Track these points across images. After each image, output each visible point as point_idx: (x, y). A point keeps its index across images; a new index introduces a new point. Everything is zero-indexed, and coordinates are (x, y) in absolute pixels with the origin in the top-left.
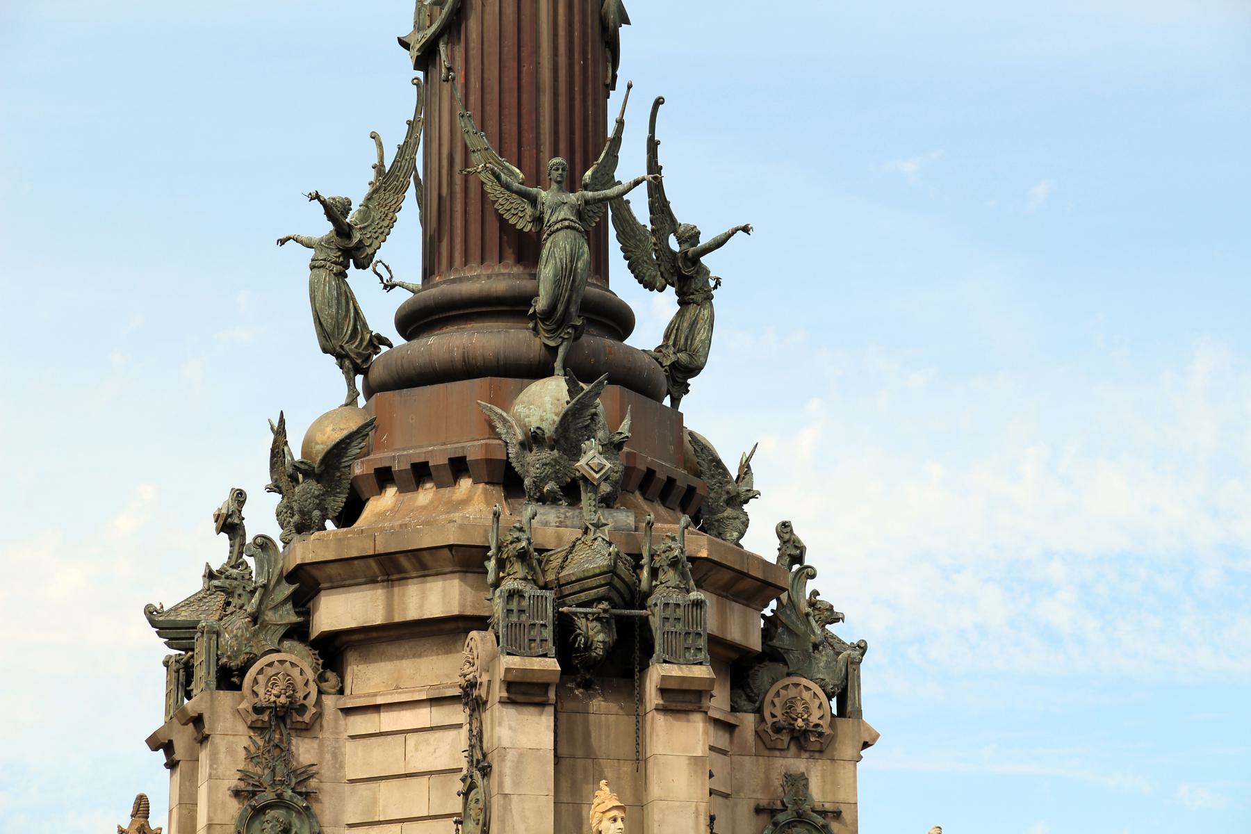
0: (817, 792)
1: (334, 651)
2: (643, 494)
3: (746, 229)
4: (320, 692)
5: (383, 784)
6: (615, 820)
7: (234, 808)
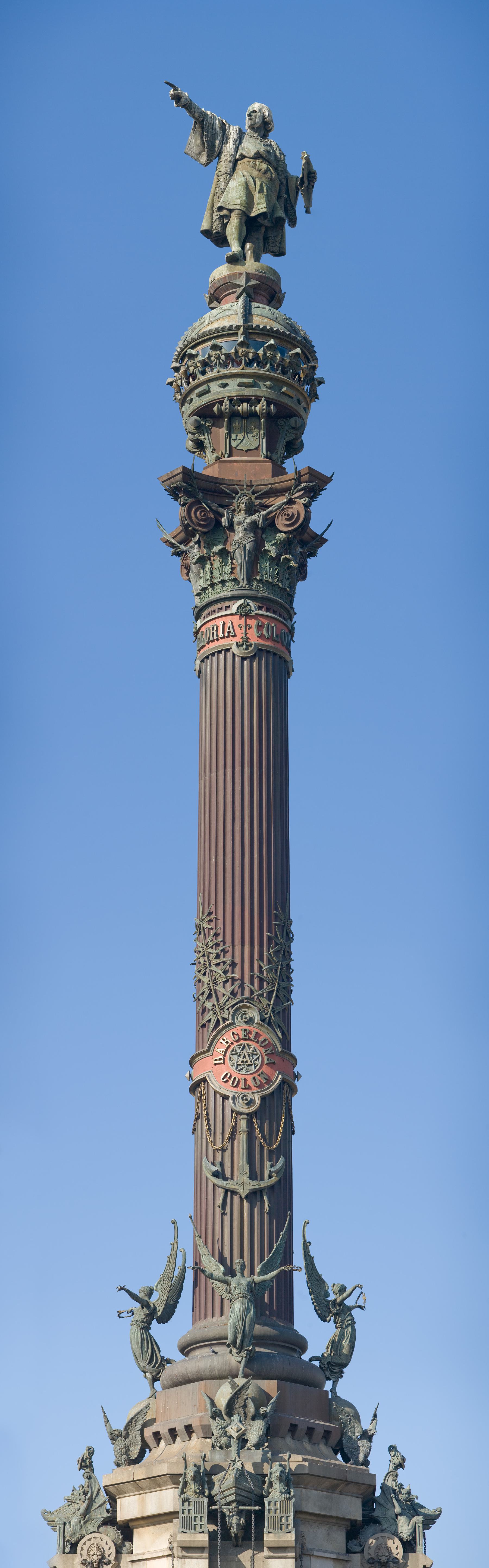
2: (293, 1437)
4: (118, 1552)
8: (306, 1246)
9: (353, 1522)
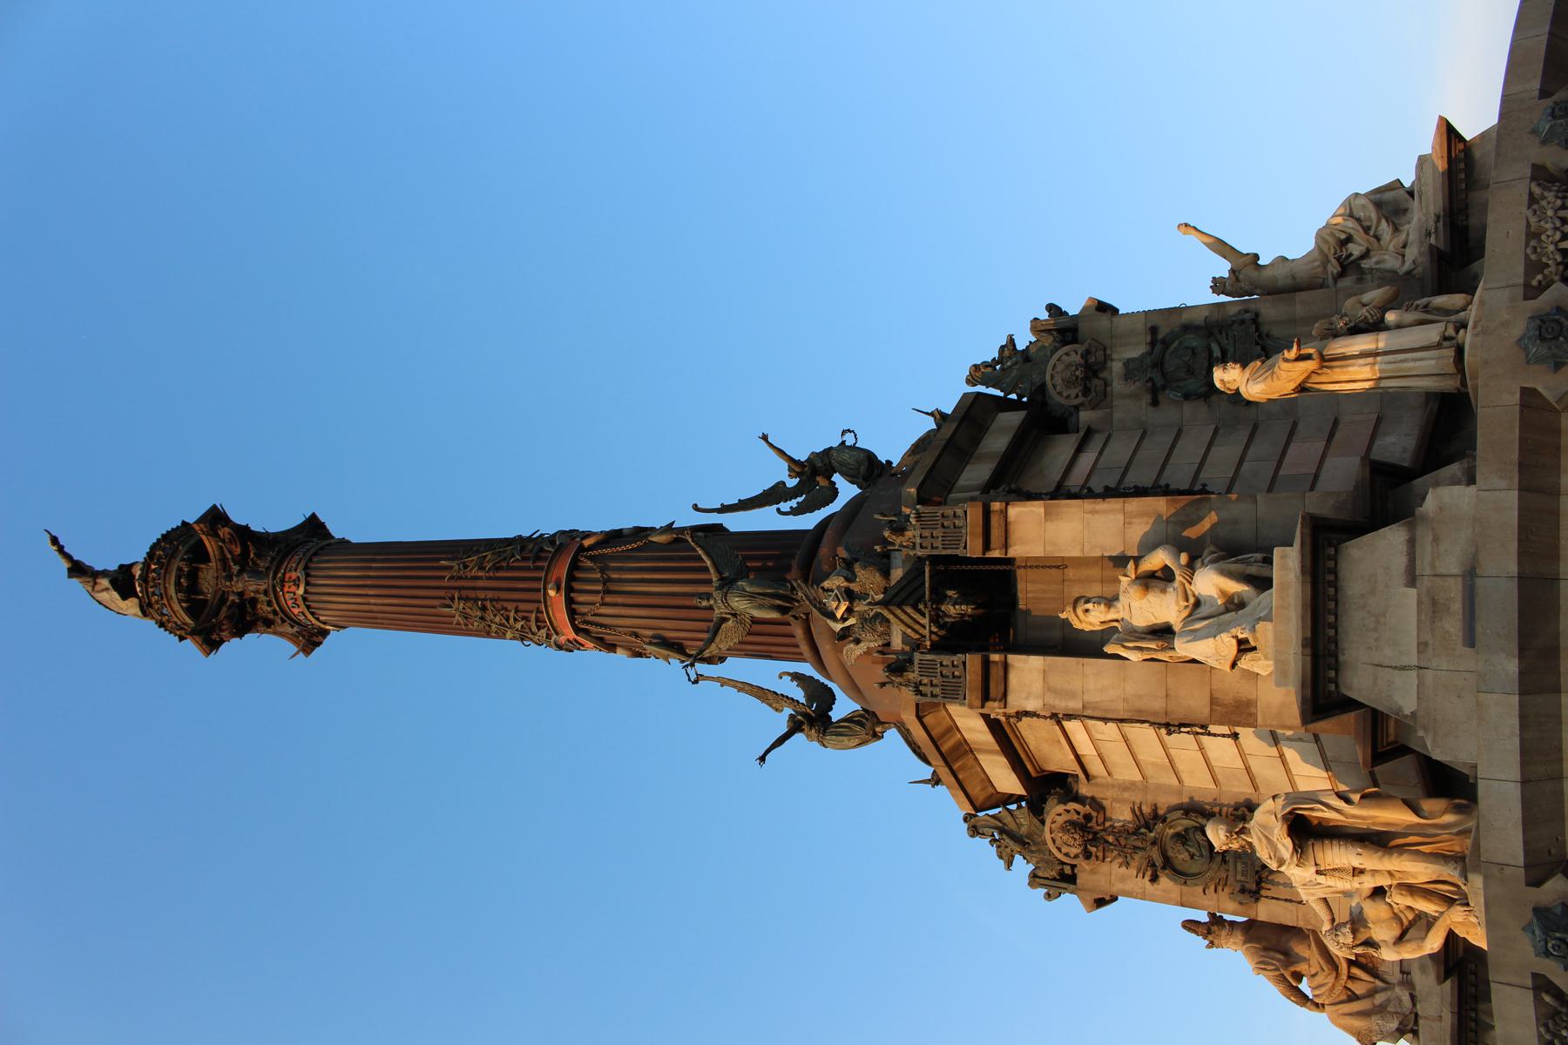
0: (1136, 352)
3: (765, 438)
4: (1077, 798)
5: (1140, 757)
6: (1087, 611)
7: (1165, 881)
8: (725, 509)
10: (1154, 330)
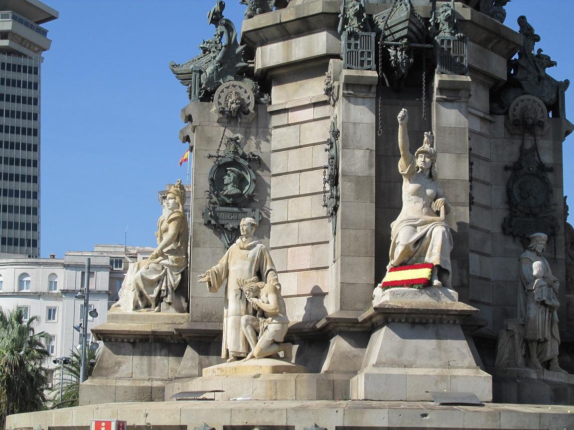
1: (266, 80)
9: (497, 81)
10: (551, 170)
